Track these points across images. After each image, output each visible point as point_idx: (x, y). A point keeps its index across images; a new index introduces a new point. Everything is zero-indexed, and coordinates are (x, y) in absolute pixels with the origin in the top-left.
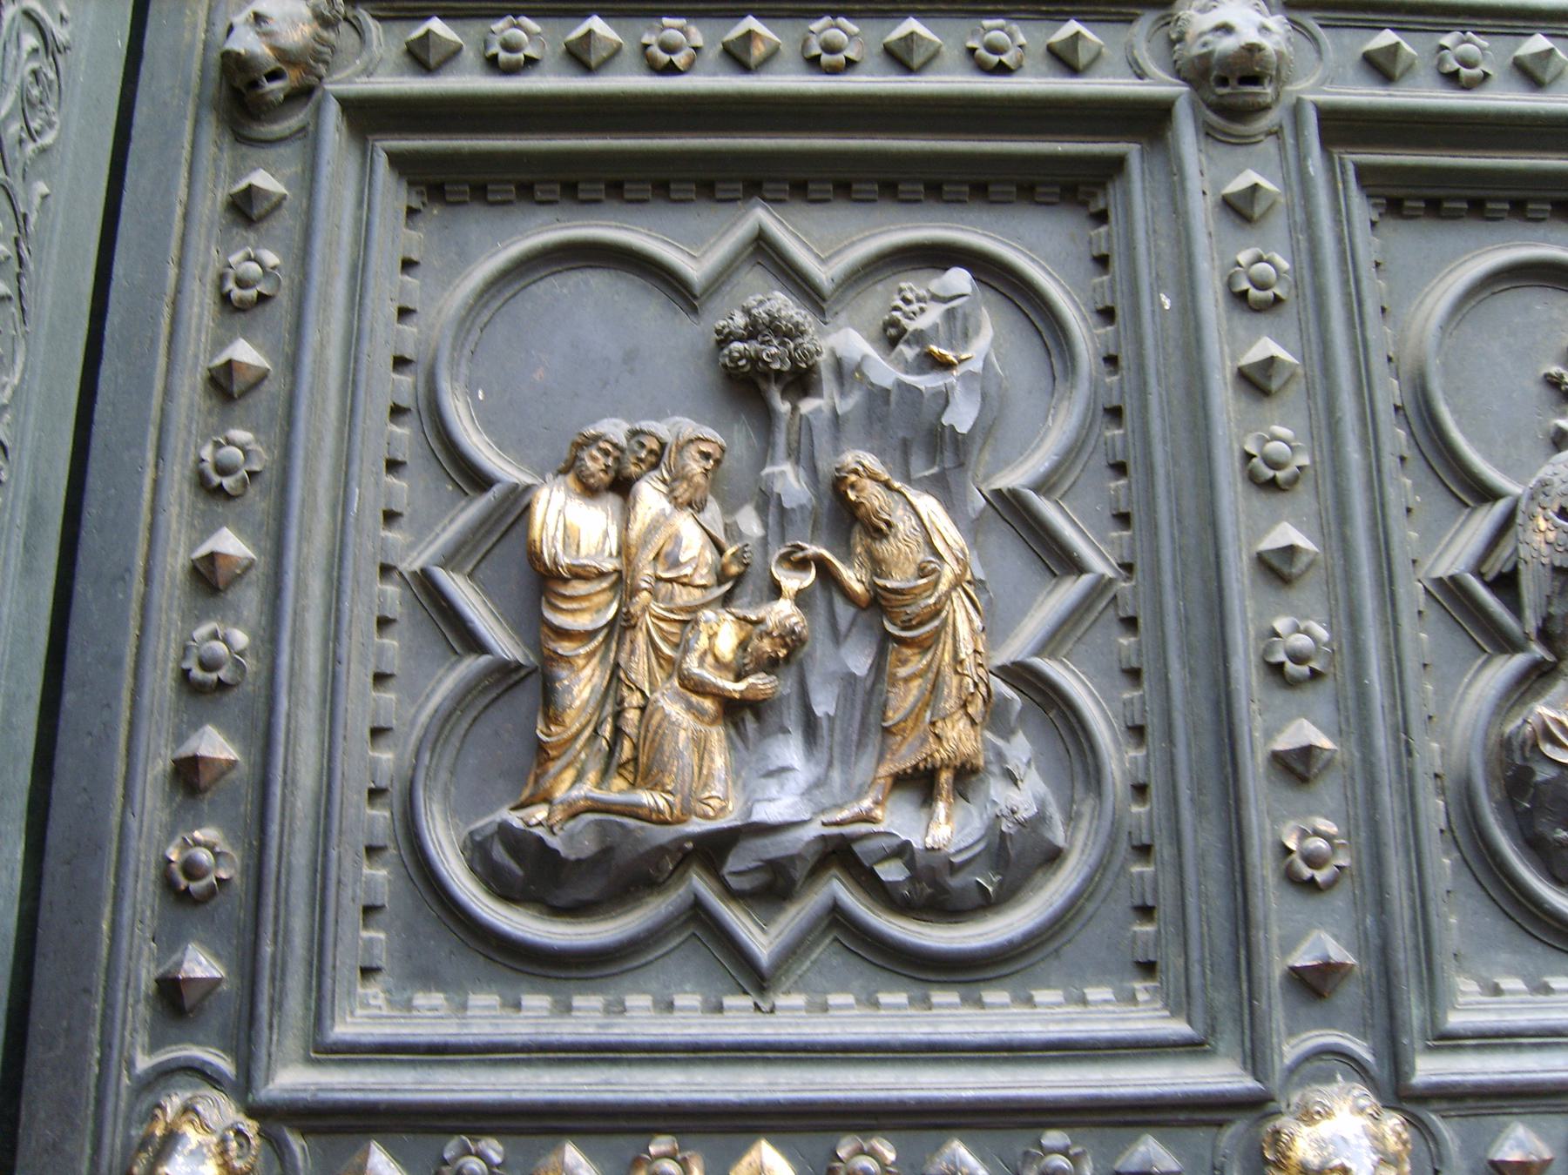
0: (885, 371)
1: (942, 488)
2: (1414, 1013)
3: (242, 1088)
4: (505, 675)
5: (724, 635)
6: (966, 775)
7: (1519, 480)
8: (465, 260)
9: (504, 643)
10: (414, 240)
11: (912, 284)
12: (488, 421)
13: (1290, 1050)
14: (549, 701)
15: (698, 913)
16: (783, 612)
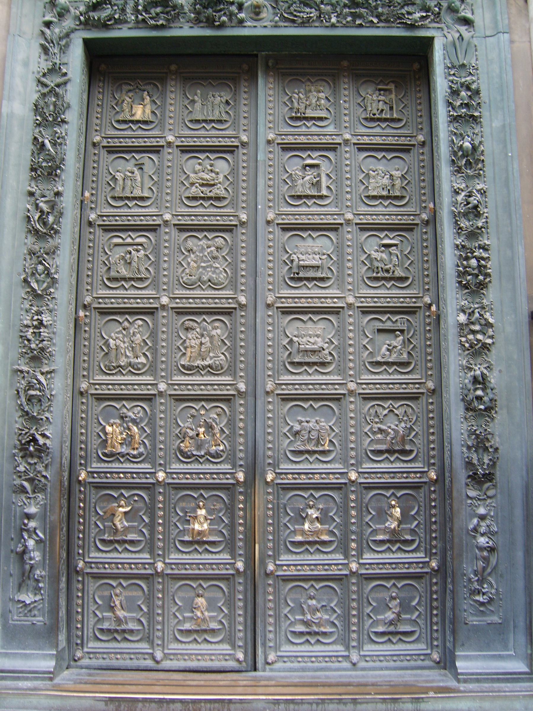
0: (133, 416)
1: (137, 426)
2: (168, 466)
3: (86, 470)
4: (104, 440)
5: (119, 437)
6: (137, 449)
7: (184, 424)
8: (100, 405)
9: (104, 438)
10: (96, 404)
11: (135, 408)
12: (103, 420)
13: (158, 469)
14: (107, 442)
15: (118, 458)
16: (124, 436)
